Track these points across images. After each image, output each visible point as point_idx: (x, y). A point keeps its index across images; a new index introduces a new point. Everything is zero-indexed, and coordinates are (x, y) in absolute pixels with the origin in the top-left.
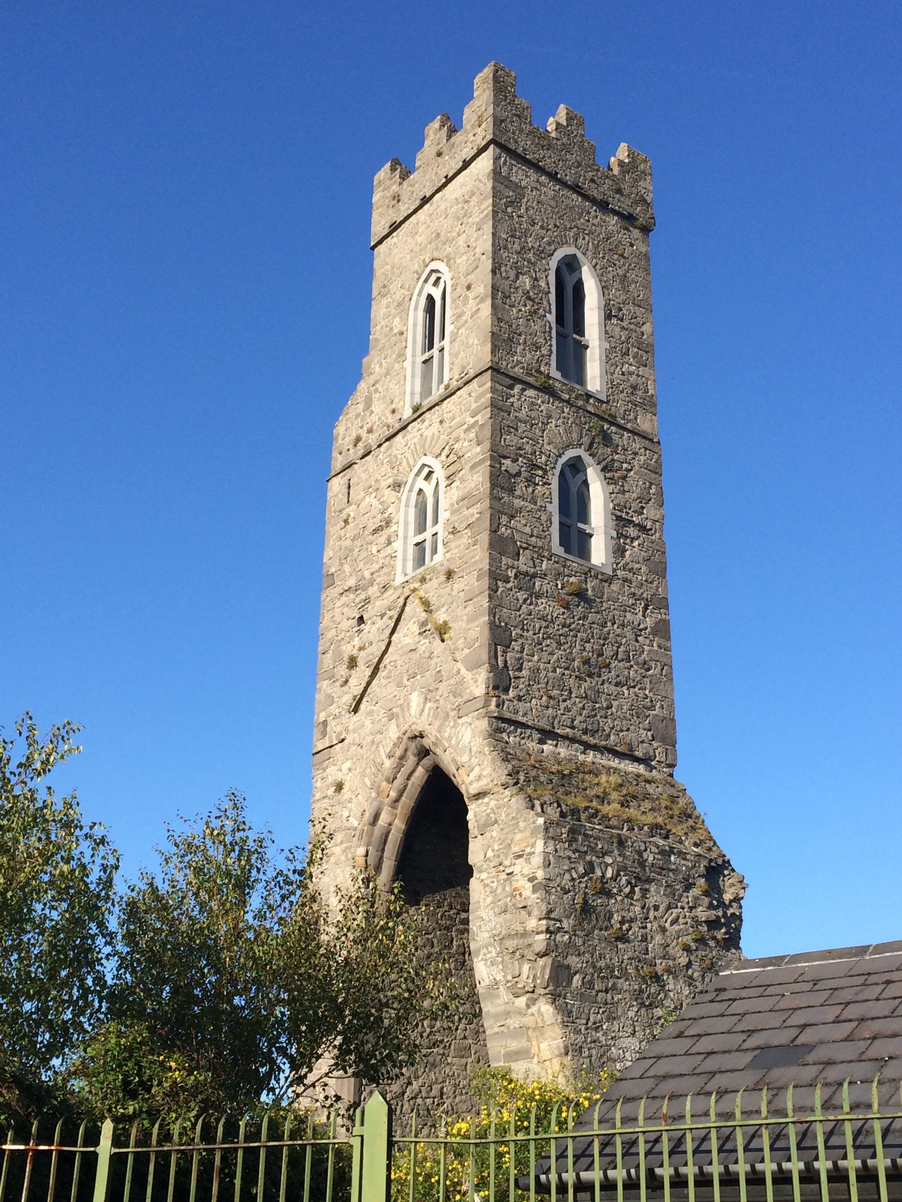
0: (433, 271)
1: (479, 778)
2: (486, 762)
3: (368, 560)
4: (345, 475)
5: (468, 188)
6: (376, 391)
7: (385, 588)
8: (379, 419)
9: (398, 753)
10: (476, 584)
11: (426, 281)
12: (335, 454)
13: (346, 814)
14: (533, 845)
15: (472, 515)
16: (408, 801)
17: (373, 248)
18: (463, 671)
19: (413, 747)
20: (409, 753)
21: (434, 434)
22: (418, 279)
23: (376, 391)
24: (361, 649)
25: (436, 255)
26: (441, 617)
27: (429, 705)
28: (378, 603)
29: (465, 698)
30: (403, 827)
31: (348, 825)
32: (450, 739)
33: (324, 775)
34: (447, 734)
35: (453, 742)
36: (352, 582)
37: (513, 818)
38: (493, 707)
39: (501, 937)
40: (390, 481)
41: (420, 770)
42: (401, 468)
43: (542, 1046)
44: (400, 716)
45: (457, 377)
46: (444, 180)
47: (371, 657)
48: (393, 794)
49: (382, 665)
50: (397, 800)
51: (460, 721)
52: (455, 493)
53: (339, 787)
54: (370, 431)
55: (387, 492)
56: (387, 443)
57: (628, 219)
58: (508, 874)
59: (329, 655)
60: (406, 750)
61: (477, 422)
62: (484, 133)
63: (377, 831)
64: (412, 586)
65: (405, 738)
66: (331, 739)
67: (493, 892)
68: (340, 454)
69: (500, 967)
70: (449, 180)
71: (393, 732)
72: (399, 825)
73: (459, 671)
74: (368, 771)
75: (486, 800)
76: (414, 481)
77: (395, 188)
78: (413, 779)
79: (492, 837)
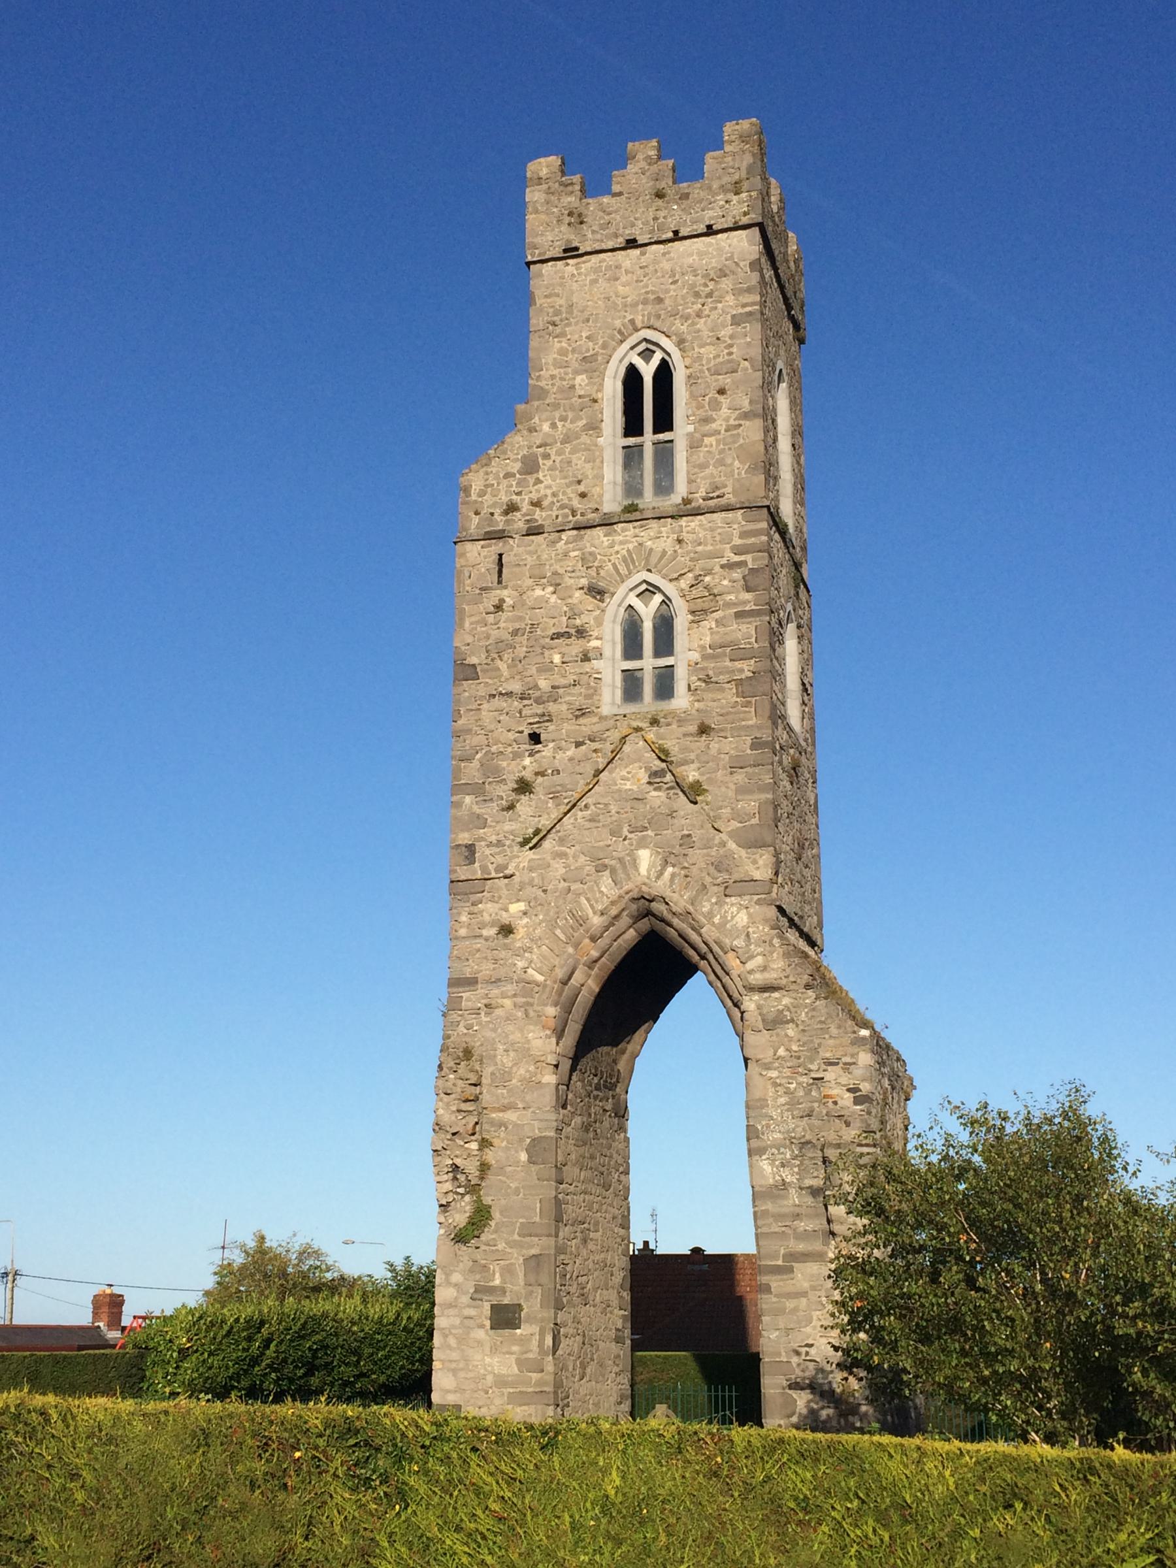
0: (645, 340)
1: (765, 968)
2: (775, 955)
4: (490, 546)
6: (546, 456)
7: (581, 713)
8: (554, 495)
9: (614, 911)
10: (749, 751)
11: (632, 348)
13: (521, 964)
15: (741, 671)
16: (608, 963)
18: (732, 845)
19: (634, 907)
20: (625, 913)
21: (664, 552)
22: (622, 342)
23: (546, 456)
24: (542, 774)
25: (653, 322)
26: (691, 774)
27: (670, 869)
29: (736, 877)
30: (597, 990)
32: (710, 915)
33: (475, 909)
35: (717, 920)
36: (516, 687)
37: (821, 1022)
39: (803, 1140)
40: (584, 582)
42: (602, 573)
44: (620, 871)
45: (702, 493)
46: (670, 235)
47: (559, 788)
48: (595, 954)
49: (582, 804)
50: (596, 961)
51: (728, 900)
52: (707, 632)
53: (507, 930)
56: (575, 532)
58: (814, 1079)
59: (476, 764)
61: (743, 564)
62: (739, 207)
64: (635, 724)
65: (627, 897)
66: (484, 869)
68: (477, 513)
69: (796, 1170)
73: (723, 844)
75: (776, 995)
76: (627, 594)
77: (571, 200)
78: (619, 940)
79: (787, 1035)
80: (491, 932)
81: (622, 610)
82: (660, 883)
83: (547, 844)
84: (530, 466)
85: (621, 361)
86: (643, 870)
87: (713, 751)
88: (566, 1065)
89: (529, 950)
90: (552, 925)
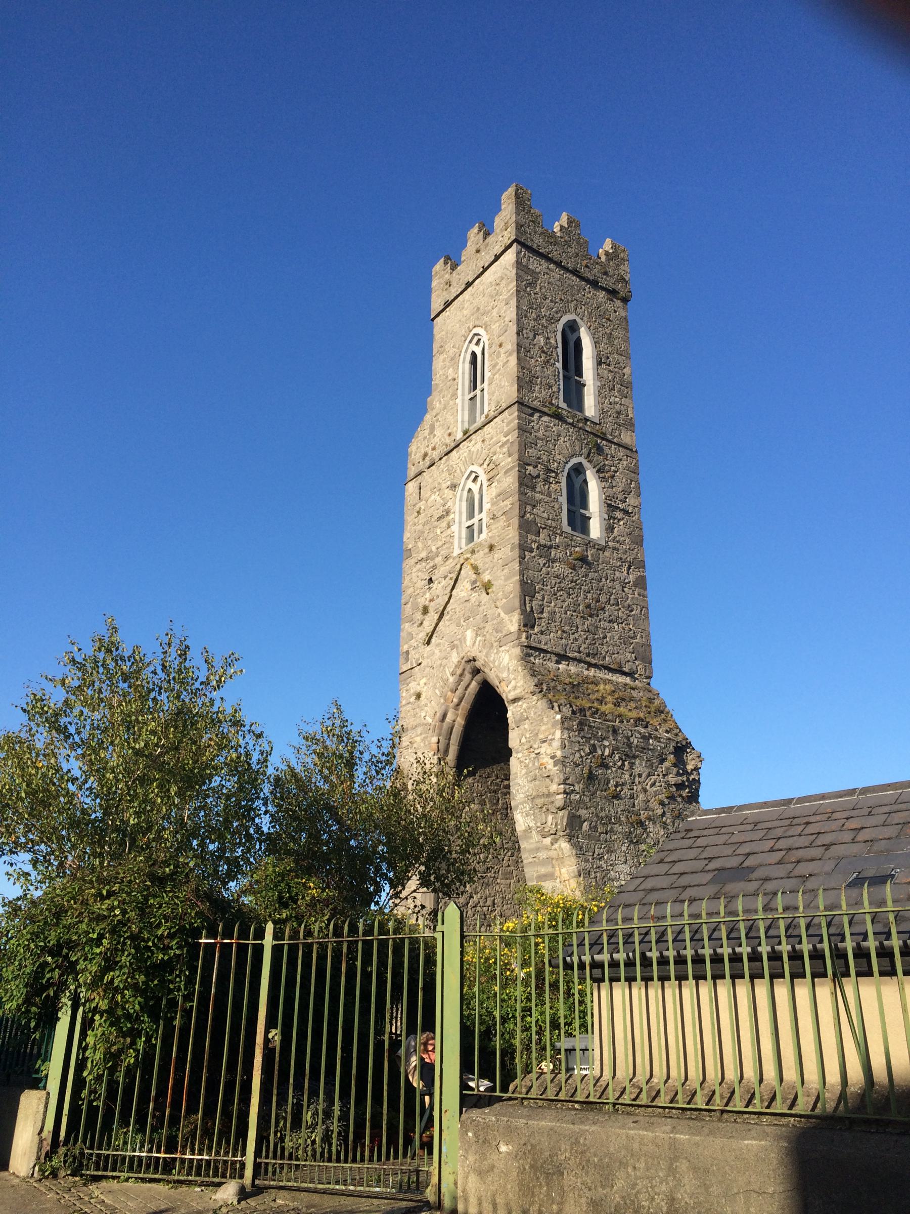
0: (475, 335)
1: (515, 688)
3: (435, 539)
5: (499, 274)
6: (437, 420)
9: (459, 672)
11: (470, 342)
12: (410, 465)
13: (423, 714)
14: (554, 734)
15: (506, 506)
16: (466, 705)
17: (433, 320)
18: (502, 614)
19: (469, 667)
20: (466, 672)
23: (437, 420)
24: (431, 600)
25: (477, 323)
26: (486, 577)
27: (479, 638)
28: (442, 569)
29: (504, 633)
31: (425, 722)
32: (494, 661)
34: (492, 659)
36: (423, 555)
38: (523, 639)
40: (449, 483)
41: (474, 683)
43: (564, 871)
45: (494, 409)
48: (456, 700)
49: (445, 612)
50: (458, 705)
51: (501, 649)
52: (494, 491)
53: (418, 696)
54: (434, 449)
55: (446, 491)
57: (612, 293)
59: (409, 605)
60: (464, 670)
62: (509, 235)
63: (445, 725)
64: (465, 556)
67: (526, 766)
70: (485, 269)
71: (455, 658)
72: (460, 722)
74: (438, 685)
75: (520, 703)
77: (447, 276)
78: (469, 690)
80: (413, 699)
81: (465, 492)
82: (475, 648)
83: (433, 640)
84: (432, 429)
85: (466, 352)
86: (468, 643)
87: (495, 560)
88: (451, 772)
89: (426, 705)
90: (435, 687)
